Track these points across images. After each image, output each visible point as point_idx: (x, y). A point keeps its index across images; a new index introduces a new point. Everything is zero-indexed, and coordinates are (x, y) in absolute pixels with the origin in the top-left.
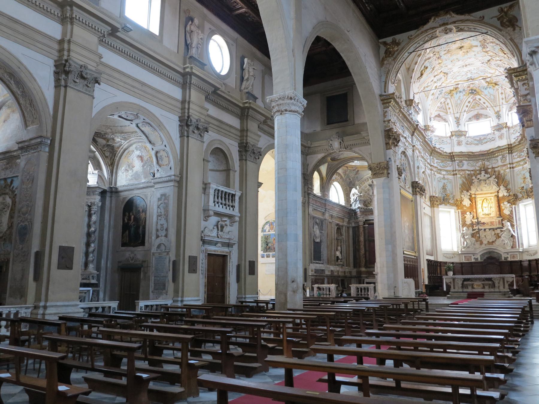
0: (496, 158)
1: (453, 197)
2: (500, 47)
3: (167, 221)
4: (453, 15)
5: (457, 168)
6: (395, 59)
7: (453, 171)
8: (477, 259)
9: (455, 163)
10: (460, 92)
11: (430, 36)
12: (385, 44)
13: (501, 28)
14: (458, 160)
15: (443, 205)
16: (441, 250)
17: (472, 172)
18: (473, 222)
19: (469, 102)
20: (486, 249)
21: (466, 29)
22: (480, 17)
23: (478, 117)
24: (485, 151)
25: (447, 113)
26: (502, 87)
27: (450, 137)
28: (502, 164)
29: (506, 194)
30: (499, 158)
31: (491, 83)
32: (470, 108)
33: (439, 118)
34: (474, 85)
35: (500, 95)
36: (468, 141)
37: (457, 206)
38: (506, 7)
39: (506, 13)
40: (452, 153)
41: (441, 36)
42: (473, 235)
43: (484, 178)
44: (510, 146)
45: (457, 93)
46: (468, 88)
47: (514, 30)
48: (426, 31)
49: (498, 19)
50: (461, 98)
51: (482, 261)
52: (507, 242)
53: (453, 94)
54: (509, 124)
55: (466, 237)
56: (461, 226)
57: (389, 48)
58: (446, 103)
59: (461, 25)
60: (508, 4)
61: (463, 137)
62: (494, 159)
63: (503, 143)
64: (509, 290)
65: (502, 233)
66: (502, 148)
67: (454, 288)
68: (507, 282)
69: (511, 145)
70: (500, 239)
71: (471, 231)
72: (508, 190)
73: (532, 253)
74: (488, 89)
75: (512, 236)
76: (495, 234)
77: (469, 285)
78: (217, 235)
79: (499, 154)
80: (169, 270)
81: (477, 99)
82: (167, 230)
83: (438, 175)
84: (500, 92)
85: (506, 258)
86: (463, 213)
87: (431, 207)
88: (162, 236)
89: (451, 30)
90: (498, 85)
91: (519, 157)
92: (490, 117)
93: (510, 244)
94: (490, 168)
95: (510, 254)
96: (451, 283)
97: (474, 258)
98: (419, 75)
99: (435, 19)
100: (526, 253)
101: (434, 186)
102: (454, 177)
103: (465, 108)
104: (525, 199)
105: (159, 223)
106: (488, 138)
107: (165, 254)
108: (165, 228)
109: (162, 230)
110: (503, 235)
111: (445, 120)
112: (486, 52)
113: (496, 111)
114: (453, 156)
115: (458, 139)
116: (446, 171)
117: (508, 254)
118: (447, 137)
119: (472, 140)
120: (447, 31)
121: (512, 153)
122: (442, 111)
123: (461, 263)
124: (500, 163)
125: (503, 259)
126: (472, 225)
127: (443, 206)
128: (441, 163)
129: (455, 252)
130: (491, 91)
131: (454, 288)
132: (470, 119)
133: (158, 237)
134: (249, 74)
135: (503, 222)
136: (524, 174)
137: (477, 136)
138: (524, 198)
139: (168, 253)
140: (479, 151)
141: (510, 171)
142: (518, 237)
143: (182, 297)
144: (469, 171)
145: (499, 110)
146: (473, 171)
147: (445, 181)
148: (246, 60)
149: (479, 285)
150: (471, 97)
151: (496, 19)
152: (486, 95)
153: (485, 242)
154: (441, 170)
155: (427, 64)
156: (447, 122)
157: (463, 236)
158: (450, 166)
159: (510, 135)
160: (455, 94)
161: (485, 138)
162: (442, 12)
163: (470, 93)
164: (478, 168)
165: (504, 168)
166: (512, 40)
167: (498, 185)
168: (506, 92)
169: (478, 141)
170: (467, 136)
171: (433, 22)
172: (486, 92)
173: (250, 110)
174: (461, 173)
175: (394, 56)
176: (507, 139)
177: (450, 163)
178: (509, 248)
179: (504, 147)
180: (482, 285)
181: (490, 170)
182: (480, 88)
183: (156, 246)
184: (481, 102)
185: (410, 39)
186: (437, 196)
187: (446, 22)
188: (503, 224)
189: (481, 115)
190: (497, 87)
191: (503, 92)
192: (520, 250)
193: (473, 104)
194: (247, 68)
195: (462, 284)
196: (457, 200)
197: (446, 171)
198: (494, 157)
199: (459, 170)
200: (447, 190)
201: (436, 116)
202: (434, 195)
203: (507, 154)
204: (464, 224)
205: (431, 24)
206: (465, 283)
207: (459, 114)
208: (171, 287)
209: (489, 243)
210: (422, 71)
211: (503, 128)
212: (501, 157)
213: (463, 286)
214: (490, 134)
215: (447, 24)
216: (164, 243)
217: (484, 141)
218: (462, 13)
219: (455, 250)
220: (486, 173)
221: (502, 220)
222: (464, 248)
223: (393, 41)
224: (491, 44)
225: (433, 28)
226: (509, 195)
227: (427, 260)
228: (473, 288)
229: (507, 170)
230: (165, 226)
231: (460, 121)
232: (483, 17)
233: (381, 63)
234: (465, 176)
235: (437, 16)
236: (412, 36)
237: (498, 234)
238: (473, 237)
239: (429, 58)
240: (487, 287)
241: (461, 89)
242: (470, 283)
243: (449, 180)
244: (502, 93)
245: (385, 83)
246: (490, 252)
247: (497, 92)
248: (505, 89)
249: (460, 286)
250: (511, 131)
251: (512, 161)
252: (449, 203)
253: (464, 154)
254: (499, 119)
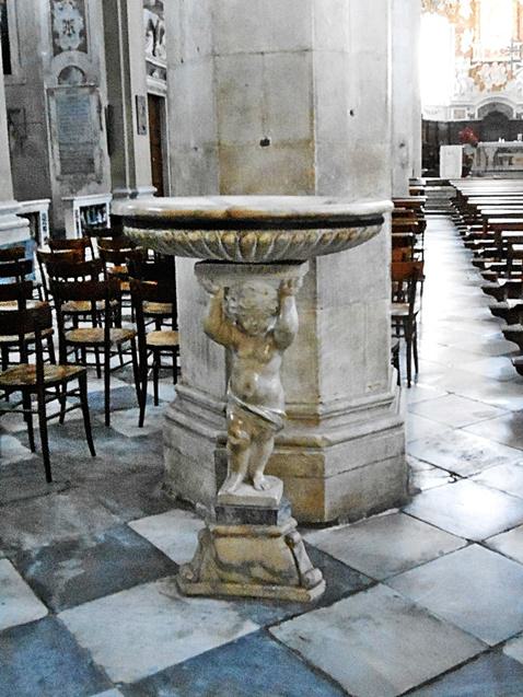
3: (82, 13)
8: (472, 116)
20: (488, 99)
37: (450, 16)
42: (471, 73)
51: (481, 119)
67: (479, 165)
77: (506, 158)
78: (153, 52)
80: (102, 129)
82: (83, 33)
86: (459, 31)
88: (70, 49)
96: (473, 155)
105: (59, 17)
107: (87, 90)
108: (78, 31)
109: (69, 35)
123: (449, 123)
125: (514, 116)
131: (479, 165)
133: (57, 50)
139: (93, 89)
143: (133, 185)
153: (488, 86)
183: (57, 74)
204: (459, 52)
206: (500, 155)
208: (105, 165)
213: (495, 164)
216: (80, 67)
222: (456, 95)
228: (510, 164)
230: (78, 25)
238: (470, 75)
242: (508, 155)
246: (494, 105)
249: (491, 159)
252: (436, 10)
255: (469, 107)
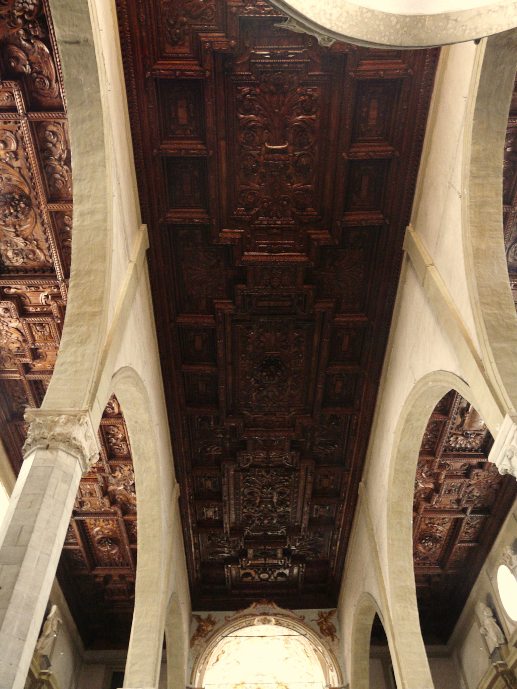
2: (303, 648)
4: (275, 606)
6: (207, 641)
11: (248, 622)
12: (198, 618)
13: (321, 635)
21: (285, 624)
22: (301, 617)
38: (326, 613)
39: (326, 620)
41: (258, 625)
47: (333, 640)
48: (245, 616)
49: (319, 624)
57: (202, 626)
59: (282, 620)
60: (328, 610)
89: (269, 622)
98: (215, 661)
99: (256, 605)
112: (287, 648)
120: (265, 622)
134: (52, 627)
148: (54, 608)
151: (316, 623)
155: (225, 648)
162: (264, 600)
166: (331, 651)
171: (254, 608)
173: (45, 686)
175: (208, 637)
185: (228, 621)
187: (267, 612)
194: (51, 619)
205: (250, 610)
215: (268, 614)
218: (284, 607)
223: (208, 617)
224: (296, 642)
225: (253, 615)
232: (304, 617)
233: (192, 643)
235: (259, 602)
236: (229, 617)
239: (229, 642)
245: (193, 671)
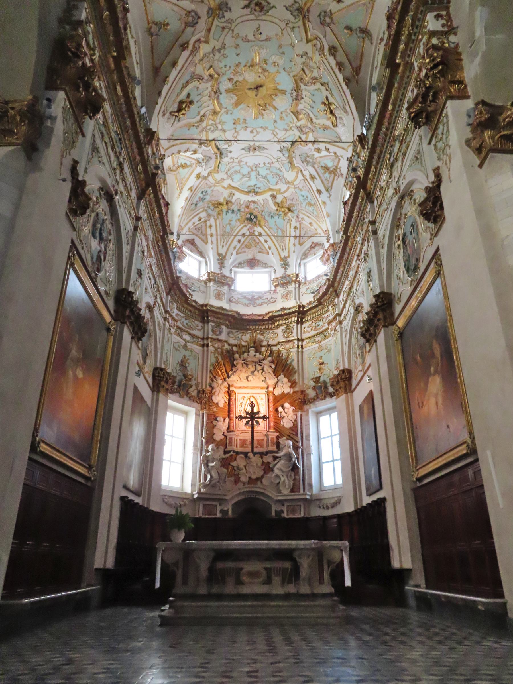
0: (275, 331)
1: (197, 385)
5: (211, 335)
7: (203, 339)
9: (208, 327)
10: (233, 211)
14: (214, 322)
15: (178, 394)
16: (160, 485)
17: (235, 349)
18: (226, 437)
19: (244, 235)
23: (252, 263)
24: (260, 316)
25: (206, 243)
26: (298, 217)
27: (206, 283)
28: (285, 340)
29: (287, 390)
30: (280, 331)
31: (282, 207)
32: (243, 246)
33: (192, 246)
34: (256, 206)
35: (293, 230)
36: (233, 297)
37: (201, 403)
40: (206, 305)
42: (225, 463)
43: (255, 359)
44: (301, 309)
45: (227, 212)
46: (246, 210)
50: (233, 223)
52: (284, 481)
53: (222, 211)
54: (301, 278)
55: (211, 464)
56: (204, 441)
58: (208, 223)
61: (226, 288)
62: (271, 331)
63: (291, 304)
64: (333, 590)
65: (276, 462)
66: (288, 311)
68: (329, 563)
69: (304, 307)
70: (271, 475)
71: (220, 454)
72: (293, 384)
73: (329, 502)
74: (276, 218)
75: (294, 468)
76: (263, 463)
79: (281, 322)
81: (257, 234)
83: (176, 338)
84: (293, 225)
85: (279, 513)
87: (153, 391)
90: (292, 211)
91: (315, 329)
92: (271, 267)
93: (290, 484)
94: (264, 346)
95: (286, 504)
96: (176, 564)
97: (222, 511)
100: (318, 503)
101: (165, 351)
102: (203, 351)
103: (235, 243)
104: (322, 399)
106: (265, 297)
110: (277, 466)
111: (201, 254)
112: (296, 114)
113: (282, 256)
114: (208, 311)
115: (218, 289)
116: (192, 336)
117: (283, 505)
118: (199, 280)
119: (239, 297)
121: (302, 323)
122: (199, 237)
124: (281, 339)
125: (273, 514)
126: (225, 442)
127: (176, 396)
128: (183, 320)
129: (186, 494)
130: (279, 221)
131: (185, 582)
132: (240, 264)
135: (280, 440)
136: (321, 358)
137: (248, 293)
138: (318, 398)
140: (250, 313)
141: (298, 352)
142: (303, 470)
144: (229, 345)
145: (287, 255)
146: (236, 346)
147: (187, 353)
149: (253, 575)
150: (248, 227)
152: (271, 228)
153: (243, 479)
154: (182, 330)
156: (203, 257)
157: (206, 461)
158: (199, 330)
159: (301, 294)
160: (225, 213)
161: (260, 297)
163: (247, 219)
164: (243, 343)
165: (287, 346)
167: (276, 373)
168: (302, 226)
169: (249, 299)
170: (233, 288)
172: (271, 222)
174: (216, 346)
176: (296, 299)
177: (200, 324)
178: (286, 492)
179: (291, 310)
180: (264, 573)
181: (263, 349)
182: (263, 213)
184: (262, 239)
186: (169, 371)
188: (278, 445)
189: (258, 261)
190: (290, 213)
191: (298, 226)
192: (308, 497)
193: (248, 239)
195: (211, 570)
196: (203, 391)
197: (192, 336)
198: (271, 329)
199: (214, 339)
200: (189, 369)
201: (187, 240)
202: (163, 366)
203: (295, 324)
204: (210, 439)
206: (220, 565)
207: (225, 249)
209: (251, 481)
210: (181, 103)
211: (292, 282)
212: (283, 327)
214: (269, 292)
217: (258, 302)
219: (188, 489)
220: (258, 351)
221: (278, 438)
222: (205, 486)
226: (294, 392)
227: (123, 499)
229: (291, 350)
231: (226, 262)
234: (222, 352)
237: (269, 463)
240: (277, 580)
241: (235, 208)
243: (194, 353)
244: (295, 228)
247: (288, 225)
248: (302, 219)
249: (204, 573)
250: (303, 289)
251: (301, 335)
252: (187, 394)
253: (225, 312)
254: (285, 269)
255: (222, 501)
